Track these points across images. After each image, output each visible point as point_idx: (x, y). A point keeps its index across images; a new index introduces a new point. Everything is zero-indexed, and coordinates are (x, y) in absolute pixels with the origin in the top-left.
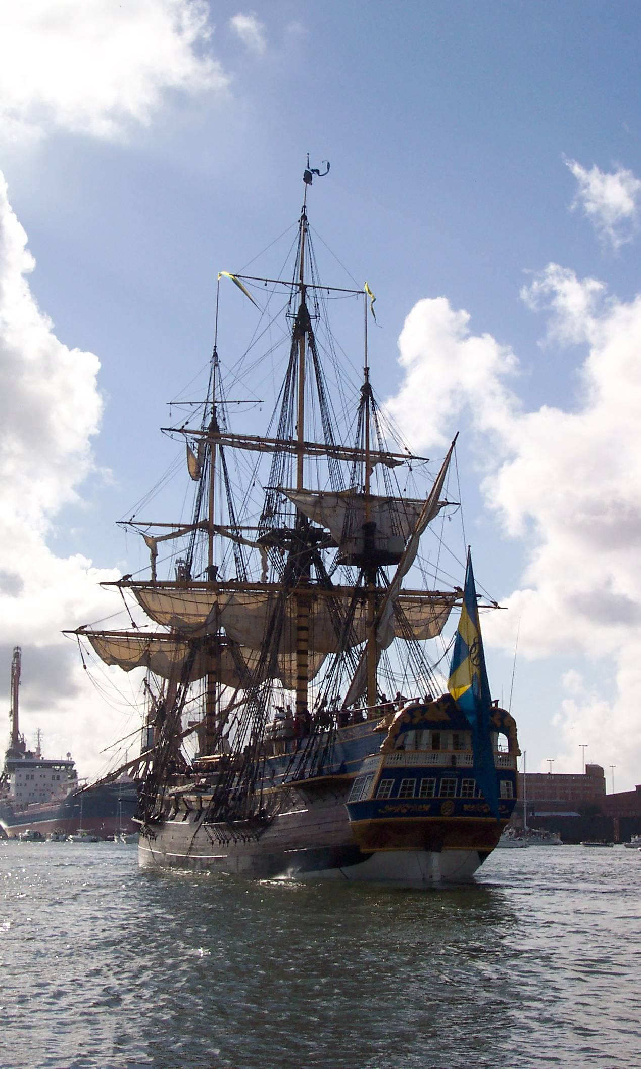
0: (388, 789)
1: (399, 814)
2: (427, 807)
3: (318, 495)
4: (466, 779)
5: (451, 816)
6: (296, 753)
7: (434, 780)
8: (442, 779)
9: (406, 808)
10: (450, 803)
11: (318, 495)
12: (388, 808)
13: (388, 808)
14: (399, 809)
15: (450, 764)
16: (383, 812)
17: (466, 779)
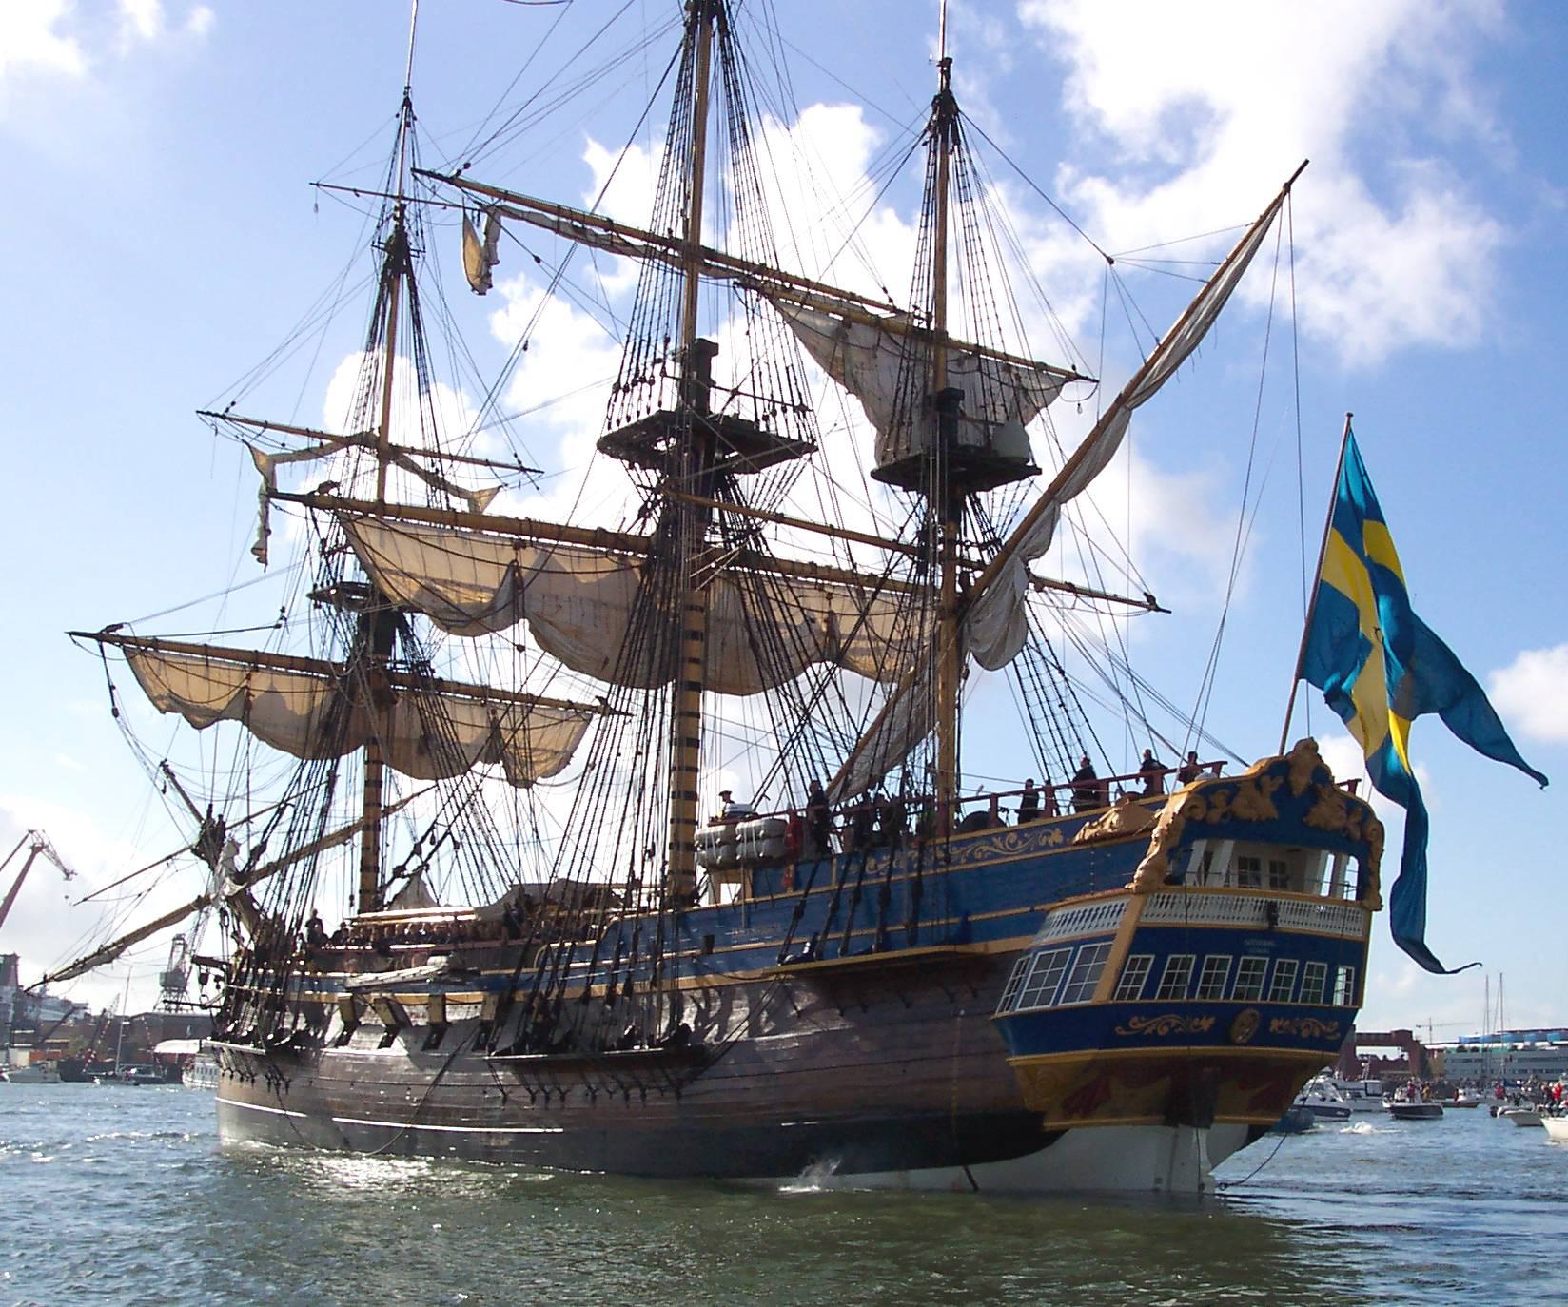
0: (1035, 982)
1: (1155, 1040)
2: (1206, 1024)
3: (841, 318)
4: (1312, 963)
5: (1250, 1043)
6: (806, 894)
7: (1191, 959)
8: (1207, 957)
9: (1169, 1024)
10: (1253, 1015)
11: (841, 318)
12: (1137, 1023)
13: (1137, 1023)
14: (1153, 1027)
15: (1266, 924)
16: (1123, 1033)
17: (1312, 963)
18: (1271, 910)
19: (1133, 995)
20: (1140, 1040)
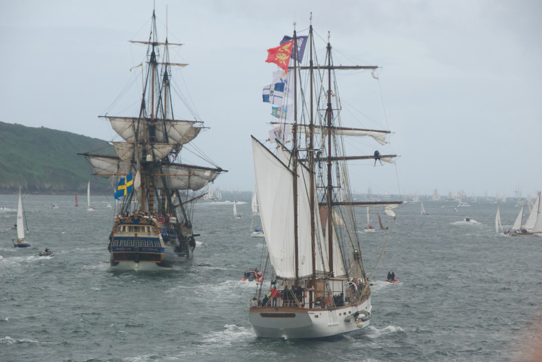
2: (130, 249)
13: (118, 249)
18: (136, 234)
19: (116, 245)
20: (118, 251)
